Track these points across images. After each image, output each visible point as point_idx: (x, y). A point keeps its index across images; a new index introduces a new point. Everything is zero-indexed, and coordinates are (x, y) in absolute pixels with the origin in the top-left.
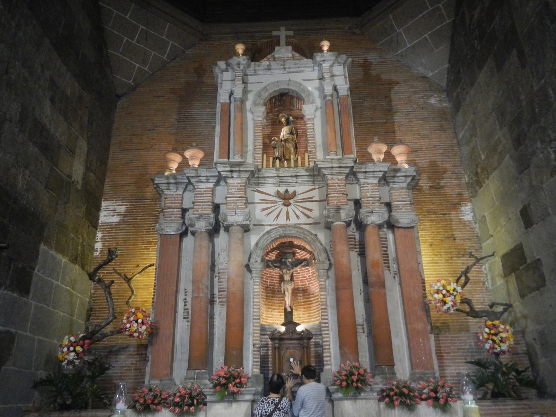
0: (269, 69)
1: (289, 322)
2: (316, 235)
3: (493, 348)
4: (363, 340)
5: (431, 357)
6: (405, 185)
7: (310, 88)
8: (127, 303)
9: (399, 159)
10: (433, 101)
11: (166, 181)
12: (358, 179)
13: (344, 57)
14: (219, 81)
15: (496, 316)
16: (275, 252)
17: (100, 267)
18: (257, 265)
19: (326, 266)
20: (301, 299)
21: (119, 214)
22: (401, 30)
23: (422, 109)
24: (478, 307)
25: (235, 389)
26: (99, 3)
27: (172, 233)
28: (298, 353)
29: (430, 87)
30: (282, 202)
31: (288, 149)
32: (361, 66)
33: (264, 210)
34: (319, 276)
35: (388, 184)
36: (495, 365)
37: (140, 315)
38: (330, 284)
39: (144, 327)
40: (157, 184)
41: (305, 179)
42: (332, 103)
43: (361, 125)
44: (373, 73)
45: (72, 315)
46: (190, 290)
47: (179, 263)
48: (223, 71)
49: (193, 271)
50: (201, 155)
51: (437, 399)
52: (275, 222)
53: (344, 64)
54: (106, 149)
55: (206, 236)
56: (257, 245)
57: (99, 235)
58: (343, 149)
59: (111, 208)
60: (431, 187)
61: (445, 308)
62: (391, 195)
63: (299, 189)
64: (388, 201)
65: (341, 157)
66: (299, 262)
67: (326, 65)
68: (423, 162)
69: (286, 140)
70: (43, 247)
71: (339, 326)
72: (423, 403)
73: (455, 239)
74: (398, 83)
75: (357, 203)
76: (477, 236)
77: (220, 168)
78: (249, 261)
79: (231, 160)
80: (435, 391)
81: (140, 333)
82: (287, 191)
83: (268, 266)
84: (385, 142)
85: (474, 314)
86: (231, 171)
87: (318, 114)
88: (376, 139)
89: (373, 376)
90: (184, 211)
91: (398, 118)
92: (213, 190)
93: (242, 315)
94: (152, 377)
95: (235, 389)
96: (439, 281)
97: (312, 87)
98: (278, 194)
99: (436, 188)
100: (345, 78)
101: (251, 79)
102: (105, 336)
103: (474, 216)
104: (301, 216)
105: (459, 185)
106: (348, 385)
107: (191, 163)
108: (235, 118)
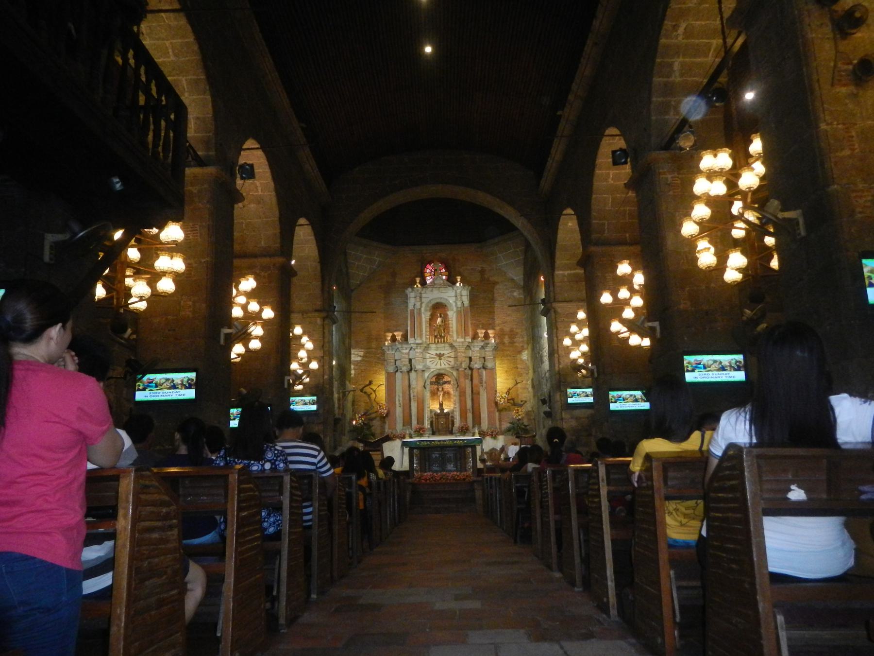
0: (432, 291)
1: (442, 409)
2: (452, 373)
3: (516, 418)
4: (470, 416)
5: (495, 421)
6: (491, 349)
7: (451, 302)
8: (375, 400)
9: (491, 335)
10: (515, 294)
12: (471, 349)
13: (467, 287)
15: (521, 406)
16: (435, 377)
17: (365, 387)
18: (428, 386)
19: (456, 386)
20: (446, 396)
21: (360, 356)
22: (500, 255)
23: (510, 298)
24: (516, 403)
25: (422, 433)
26: (347, 251)
27: (392, 371)
28: (444, 420)
29: (515, 286)
30: (438, 358)
31: (441, 330)
32: (479, 272)
33: (431, 361)
34: (453, 391)
35: (484, 349)
36: (517, 424)
37: (384, 406)
38: (457, 394)
39: (386, 411)
40: (384, 349)
41: (448, 348)
42: (461, 312)
43: (477, 308)
44: (486, 276)
46: (401, 395)
47: (395, 383)
49: (403, 388)
50: (401, 333)
51: (492, 435)
52: (435, 367)
53: (468, 289)
54: (350, 322)
55: (407, 374)
56: (428, 377)
57: (352, 367)
58: (465, 333)
59: (356, 353)
60: (510, 343)
61: (501, 403)
62: (485, 354)
63: (445, 352)
64: (484, 356)
65: (462, 340)
66: (445, 383)
67: (458, 291)
68: (507, 329)
69: (440, 326)
71: (461, 410)
72: (488, 437)
73: (518, 368)
74: (498, 283)
75: (470, 359)
76: (528, 367)
77: (412, 345)
78: (425, 383)
79: (417, 342)
80: (492, 432)
81: (384, 413)
82: (440, 354)
83: (432, 384)
84: (485, 329)
85: (514, 404)
86: (417, 347)
87: (455, 315)
88: (481, 326)
89: (474, 427)
90: (396, 360)
91: (497, 305)
92: (409, 352)
93: (423, 406)
94: (389, 429)
95: (422, 433)
96: (499, 393)
97: (452, 301)
98: (436, 355)
99: (512, 343)
100: (467, 296)
101: (424, 295)
102: (371, 414)
103: (527, 358)
104: (447, 364)
105: (523, 342)
106: (462, 431)
107: (397, 337)
108: (417, 318)
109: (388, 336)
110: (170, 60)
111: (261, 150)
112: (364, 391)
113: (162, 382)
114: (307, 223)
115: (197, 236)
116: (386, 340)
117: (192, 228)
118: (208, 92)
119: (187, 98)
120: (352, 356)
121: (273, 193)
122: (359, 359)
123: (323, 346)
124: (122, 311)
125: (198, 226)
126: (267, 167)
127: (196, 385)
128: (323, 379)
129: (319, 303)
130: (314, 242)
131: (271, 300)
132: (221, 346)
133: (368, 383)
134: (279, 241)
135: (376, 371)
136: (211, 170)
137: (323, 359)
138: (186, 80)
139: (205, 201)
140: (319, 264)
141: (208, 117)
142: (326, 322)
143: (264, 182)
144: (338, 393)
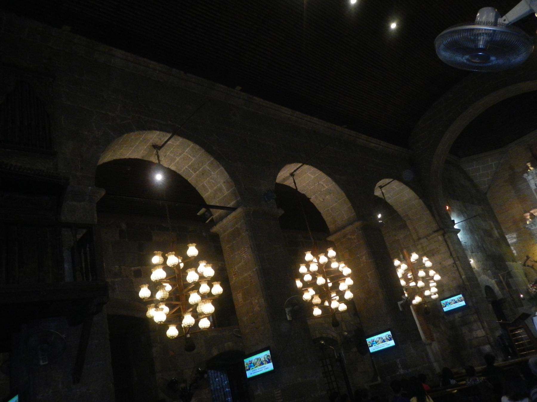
11: (530, 225)
14: (528, 180)
21: (515, 238)
26: (465, 170)
45: (522, 278)
48: (527, 176)
57: (512, 248)
59: (510, 237)
70: (507, 263)
109: (527, 216)
110: (193, 160)
111: (305, 165)
112: (526, 265)
113: (256, 362)
114: (391, 180)
115: (247, 255)
116: (527, 220)
117: (244, 251)
118: (220, 165)
119: (214, 174)
120: (509, 240)
121: (334, 183)
122: (515, 240)
123: (451, 254)
124: (188, 336)
125: (246, 248)
126: (319, 171)
127: (273, 359)
128: (462, 279)
129: (434, 226)
130: (407, 187)
131: (364, 252)
132: (290, 321)
133: (526, 258)
134: (353, 211)
135: (533, 244)
136: (239, 210)
137: (456, 264)
138: (207, 165)
139: (245, 231)
140: (421, 201)
141: (228, 179)
142: (446, 236)
143: (324, 180)
144: (494, 278)
